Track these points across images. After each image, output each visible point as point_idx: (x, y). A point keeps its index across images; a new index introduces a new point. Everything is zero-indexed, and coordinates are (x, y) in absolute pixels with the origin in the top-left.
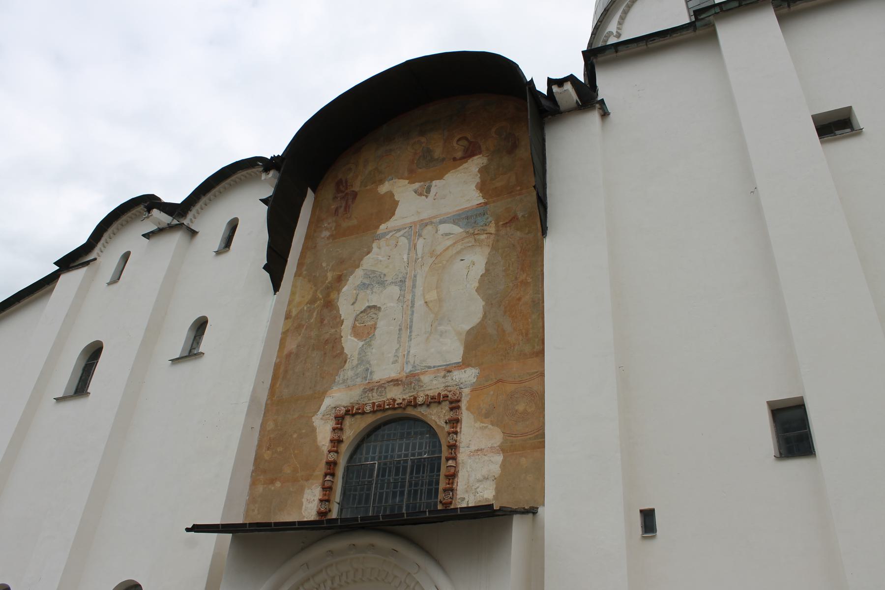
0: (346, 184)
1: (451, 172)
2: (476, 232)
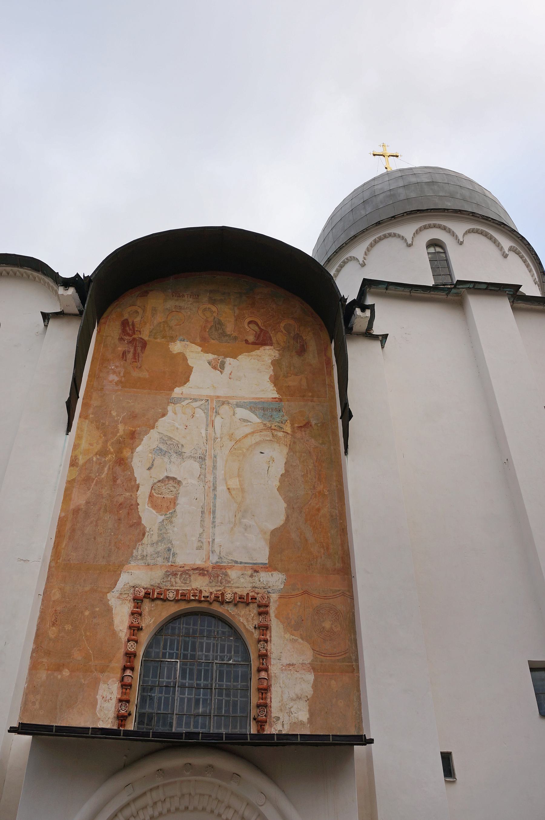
0: (134, 328)
1: (244, 354)
2: (273, 427)
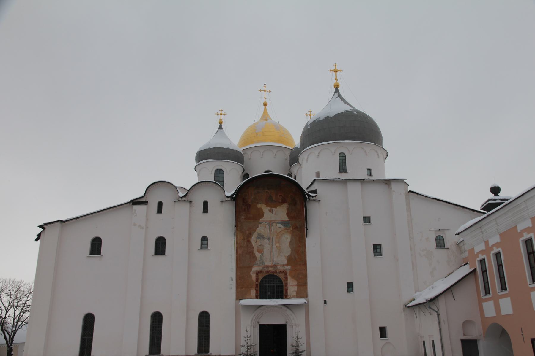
2: (287, 229)
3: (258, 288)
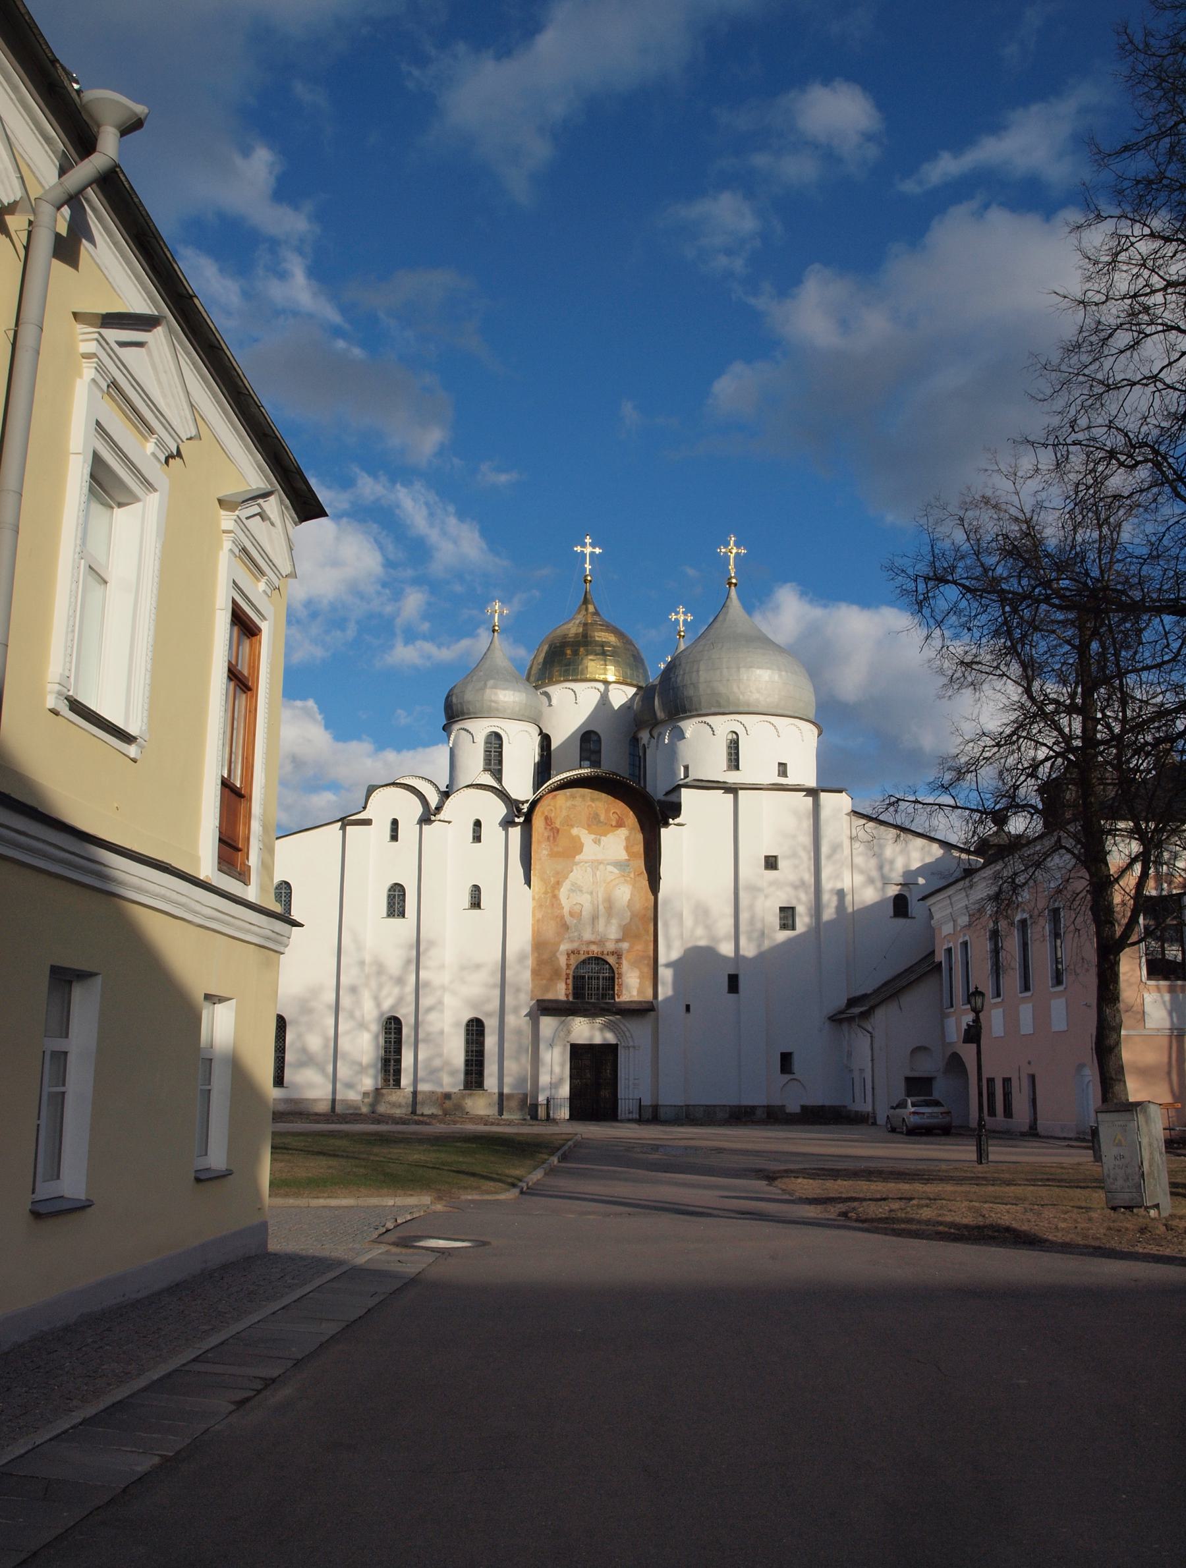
3: (570, 981)
